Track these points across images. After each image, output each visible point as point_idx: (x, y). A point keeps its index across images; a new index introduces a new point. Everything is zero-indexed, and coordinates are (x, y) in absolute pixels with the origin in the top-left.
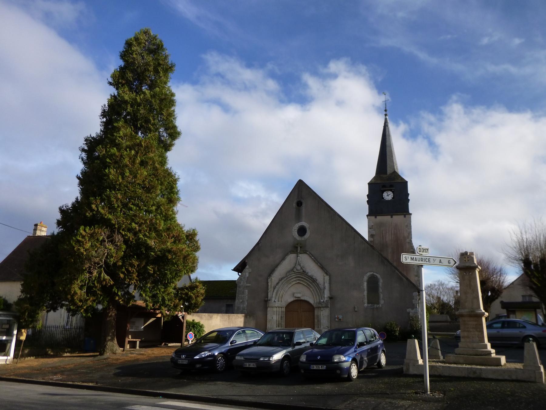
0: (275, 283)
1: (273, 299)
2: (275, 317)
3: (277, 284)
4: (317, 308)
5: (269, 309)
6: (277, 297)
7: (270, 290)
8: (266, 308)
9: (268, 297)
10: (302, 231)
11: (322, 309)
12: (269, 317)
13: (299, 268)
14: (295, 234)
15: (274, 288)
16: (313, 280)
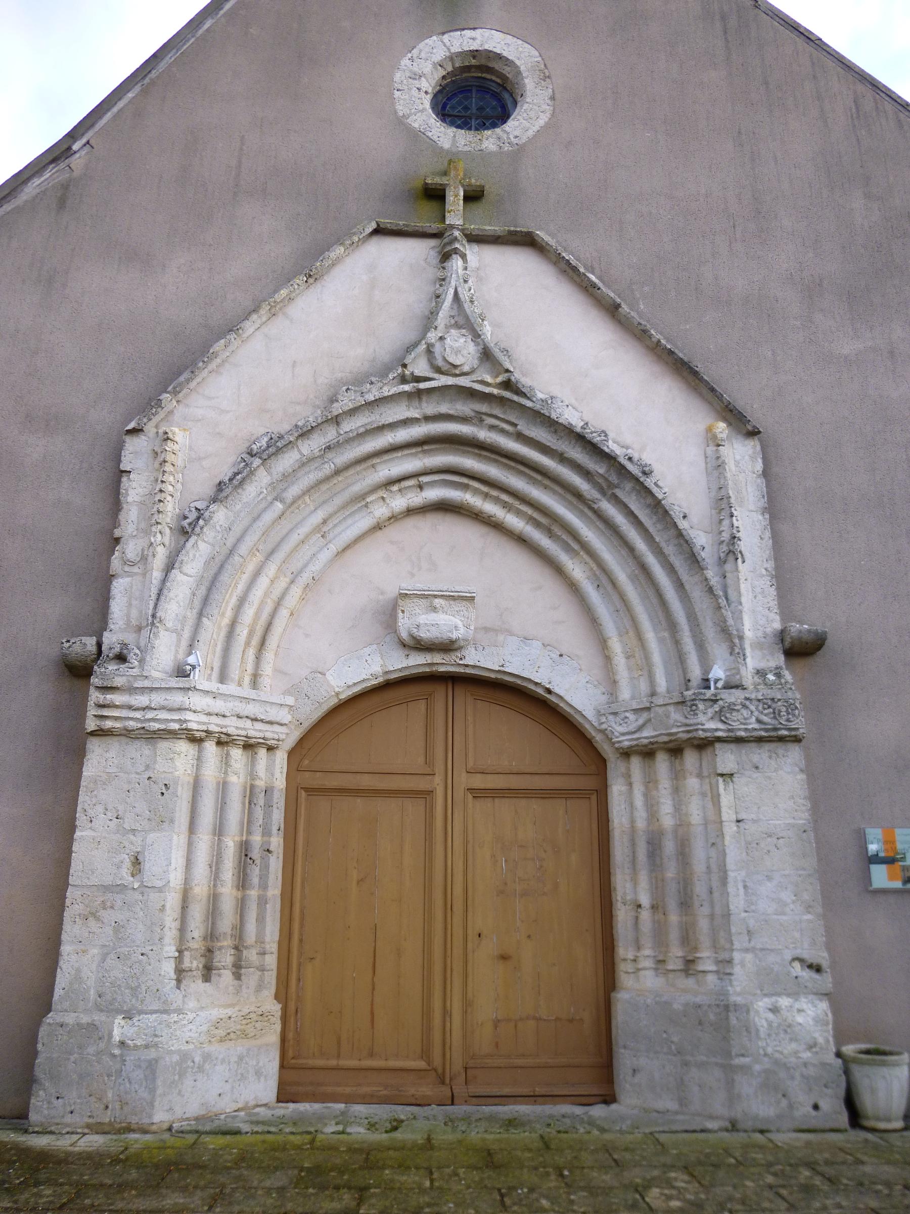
0: (201, 485)
1: (164, 651)
2: (172, 860)
3: (221, 491)
4: (625, 754)
5: (99, 759)
6: (213, 631)
7: (131, 548)
8: (67, 747)
9: (101, 619)
10: (477, 94)
11: (726, 758)
12: (94, 855)
13: (460, 349)
14: (415, 103)
15: (185, 531)
16: (614, 475)
